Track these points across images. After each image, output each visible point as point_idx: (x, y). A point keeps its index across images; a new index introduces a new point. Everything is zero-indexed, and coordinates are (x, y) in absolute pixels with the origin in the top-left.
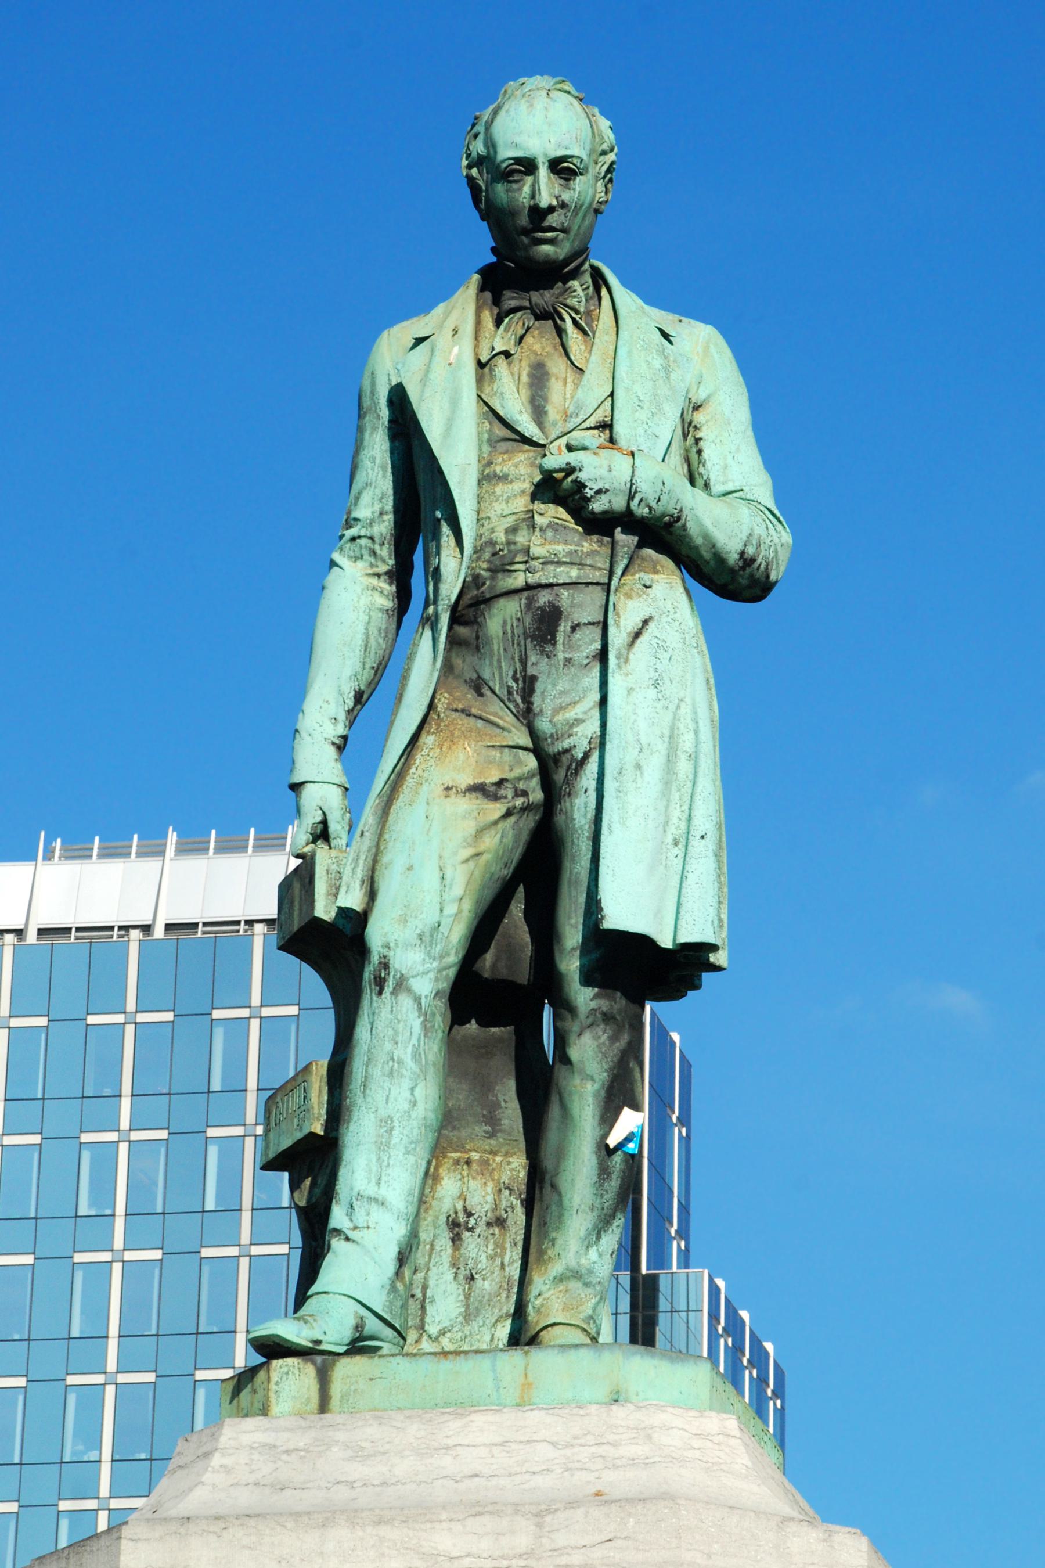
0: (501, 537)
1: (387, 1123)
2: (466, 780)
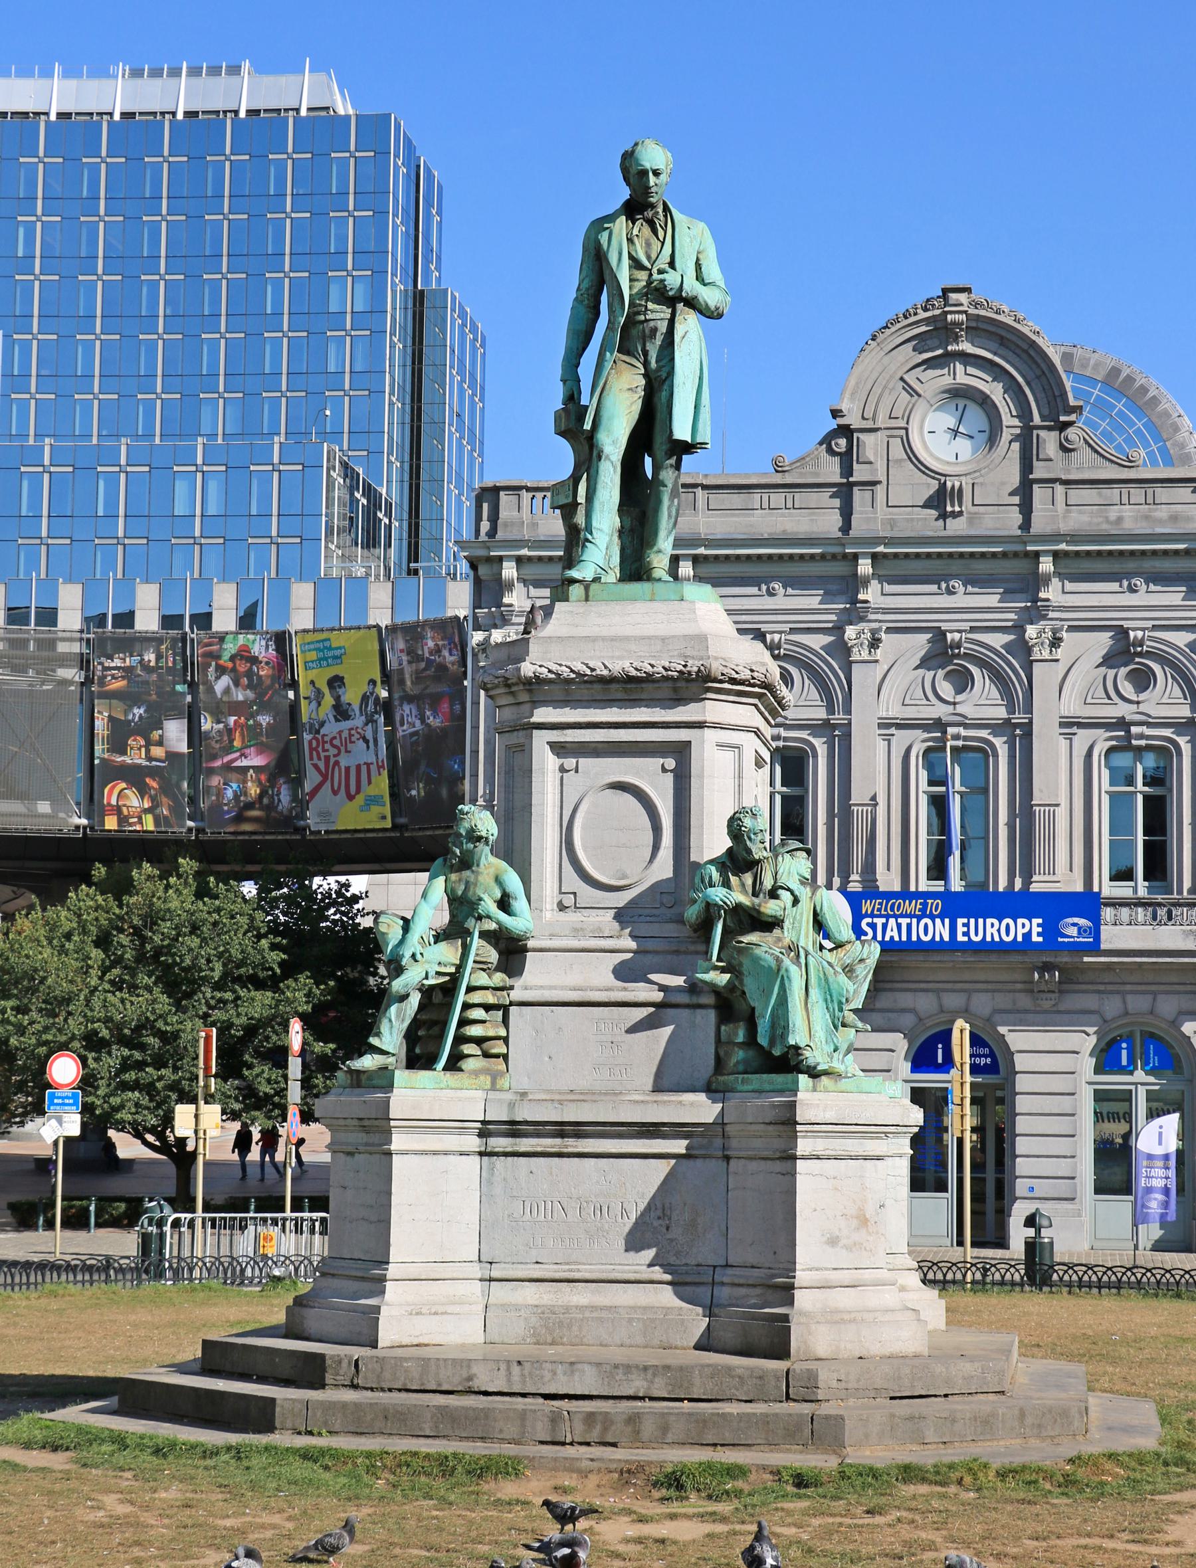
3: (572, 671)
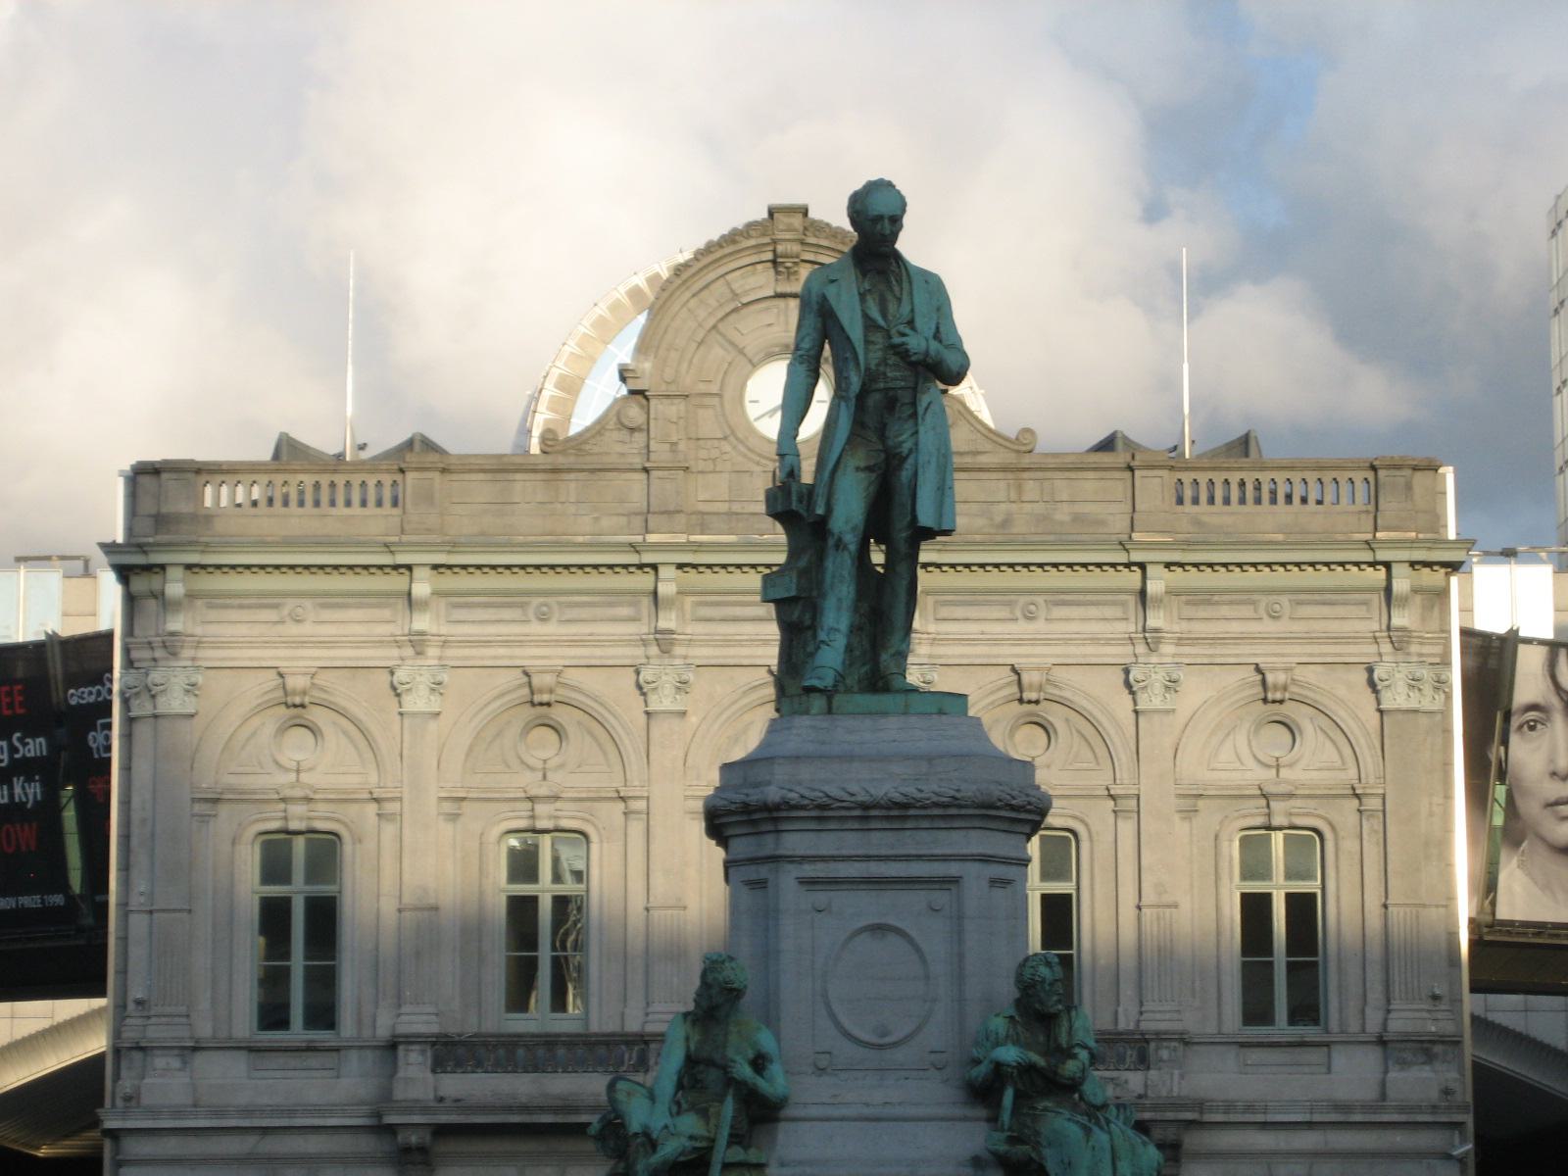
0: (873, 367)
1: (840, 600)
2: (862, 464)
3: (828, 796)
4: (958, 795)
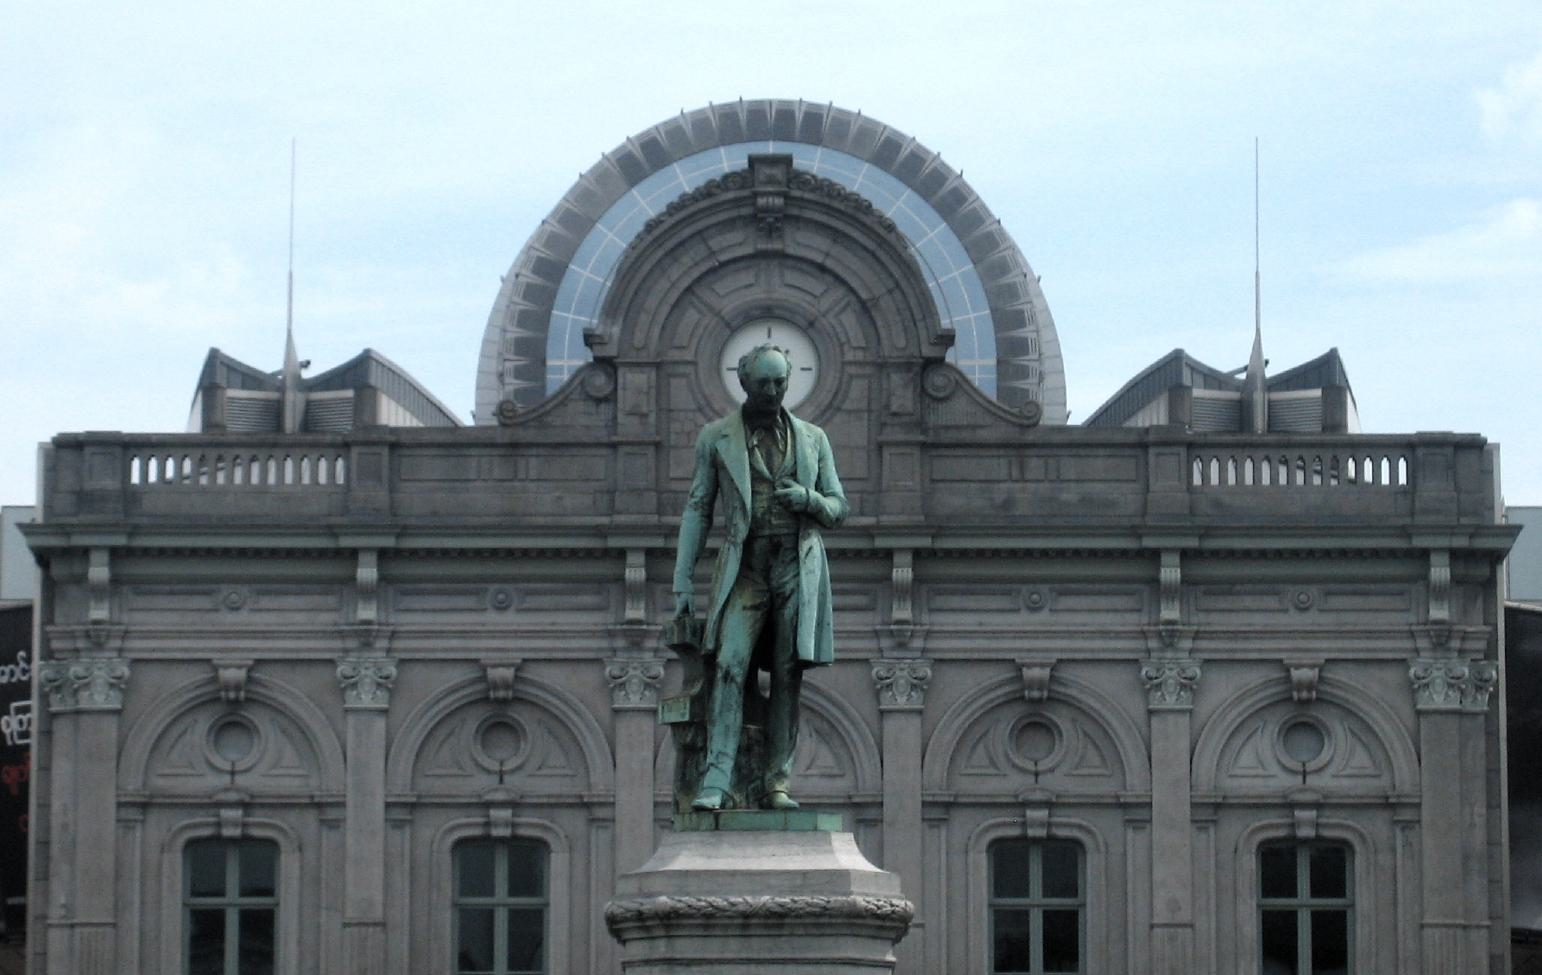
0: (759, 515)
2: (749, 604)
4: (829, 906)
